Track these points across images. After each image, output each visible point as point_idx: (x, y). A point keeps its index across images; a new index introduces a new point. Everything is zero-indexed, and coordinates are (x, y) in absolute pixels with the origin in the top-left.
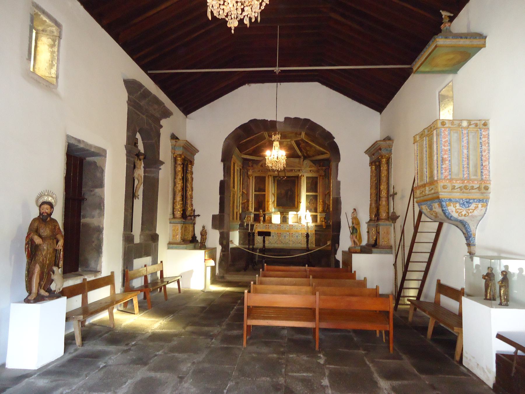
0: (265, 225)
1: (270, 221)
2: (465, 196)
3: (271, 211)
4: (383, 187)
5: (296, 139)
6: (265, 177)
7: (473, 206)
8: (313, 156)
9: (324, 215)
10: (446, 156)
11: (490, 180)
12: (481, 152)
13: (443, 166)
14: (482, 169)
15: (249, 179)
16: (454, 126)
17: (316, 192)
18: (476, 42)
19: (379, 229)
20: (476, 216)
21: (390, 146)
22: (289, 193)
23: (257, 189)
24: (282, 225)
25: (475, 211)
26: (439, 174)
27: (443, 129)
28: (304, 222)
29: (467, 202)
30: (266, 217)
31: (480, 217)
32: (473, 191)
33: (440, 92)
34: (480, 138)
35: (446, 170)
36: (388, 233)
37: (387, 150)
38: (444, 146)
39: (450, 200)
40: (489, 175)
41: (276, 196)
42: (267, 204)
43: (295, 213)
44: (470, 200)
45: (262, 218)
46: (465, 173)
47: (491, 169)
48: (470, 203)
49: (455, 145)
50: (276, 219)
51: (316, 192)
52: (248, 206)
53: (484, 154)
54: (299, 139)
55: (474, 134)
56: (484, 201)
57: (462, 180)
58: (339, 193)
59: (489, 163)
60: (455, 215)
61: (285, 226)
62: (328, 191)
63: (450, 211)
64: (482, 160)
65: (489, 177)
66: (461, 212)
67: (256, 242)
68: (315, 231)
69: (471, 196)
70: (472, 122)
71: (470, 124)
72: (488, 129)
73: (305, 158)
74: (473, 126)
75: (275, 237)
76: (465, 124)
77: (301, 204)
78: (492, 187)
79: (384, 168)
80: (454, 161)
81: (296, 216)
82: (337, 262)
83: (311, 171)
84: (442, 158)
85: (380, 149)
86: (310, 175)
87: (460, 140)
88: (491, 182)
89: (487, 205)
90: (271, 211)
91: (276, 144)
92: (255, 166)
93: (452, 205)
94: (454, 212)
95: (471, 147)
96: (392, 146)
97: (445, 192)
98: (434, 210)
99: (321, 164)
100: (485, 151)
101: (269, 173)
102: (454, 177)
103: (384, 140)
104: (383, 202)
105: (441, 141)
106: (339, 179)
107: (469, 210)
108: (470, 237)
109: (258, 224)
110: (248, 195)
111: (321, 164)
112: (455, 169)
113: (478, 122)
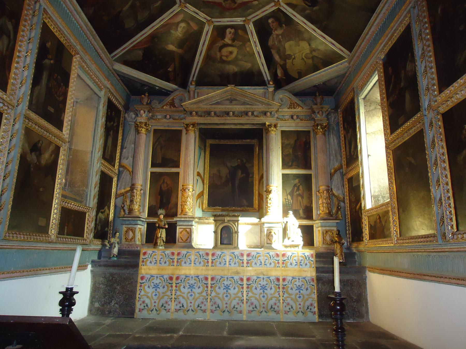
0: (168, 252)
3: (190, 214)
5: (259, 14)
6: (180, 132)
8: (301, 75)
9: (332, 225)
17: (307, 166)
22: (239, 174)
23: (159, 161)
24: (218, 252)
28: (278, 244)
30: (178, 230)
41: (207, 181)
42: (183, 195)
43: (255, 220)
45: (162, 234)
50: (204, 235)
51: (307, 166)
52: (132, 201)
54: (270, 8)
61: (227, 254)
62: (337, 165)
67: (138, 306)
68: (318, 270)
73: (279, 85)
75: (197, 290)
77: (271, 196)
81: (258, 229)
83: (292, 117)
86: (290, 126)
90: (190, 214)
92: (155, 104)
99: (319, 100)
101: (189, 120)
109: (150, 251)
110: (133, 173)
111: (319, 100)
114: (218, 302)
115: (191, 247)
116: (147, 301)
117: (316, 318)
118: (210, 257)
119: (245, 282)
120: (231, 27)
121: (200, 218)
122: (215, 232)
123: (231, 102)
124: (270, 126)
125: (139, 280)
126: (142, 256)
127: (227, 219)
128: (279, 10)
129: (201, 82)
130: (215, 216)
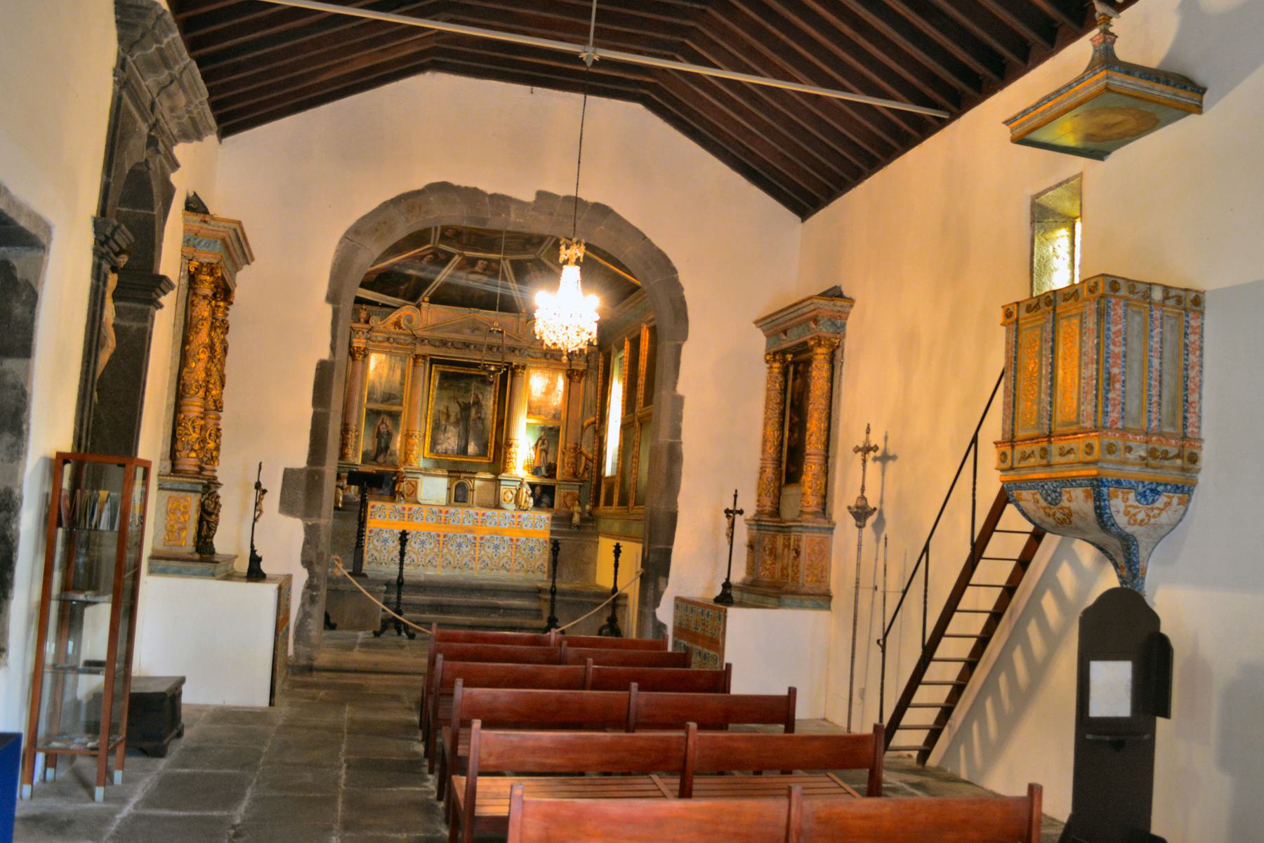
1: (412, 496)
2: (1148, 475)
4: (814, 425)
7: (1162, 500)
10: (1115, 370)
11: (1200, 440)
12: (1186, 369)
13: (1110, 395)
14: (1186, 411)
15: (354, 359)
16: (1136, 297)
18: (1184, 96)
19: (799, 540)
20: (1161, 526)
21: (843, 315)
24: (452, 510)
25: (1164, 514)
26: (1100, 415)
27: (1113, 301)
29: (1152, 490)
31: (1167, 529)
32: (1166, 463)
33: (1038, 195)
34: (1186, 334)
35: (1114, 405)
36: (823, 553)
37: (834, 324)
38: (1114, 344)
39: (1118, 482)
40: (1199, 427)
44: (1158, 484)
46: (1153, 416)
47: (1205, 414)
48: (1158, 493)
49: (1135, 344)
53: (1192, 373)
55: (1173, 322)
56: (1184, 489)
57: (1147, 434)
58: (677, 432)
59: (1200, 397)
60: (1121, 520)
63: (1113, 509)
64: (1186, 389)
65: (1199, 433)
66: (1135, 515)
67: (367, 558)
68: (552, 532)
69: (1162, 476)
70: (1172, 293)
71: (1166, 298)
72: (1202, 313)
74: (1172, 302)
75: (428, 546)
76: (1157, 295)
77: (512, 450)
78: (1206, 455)
79: (819, 373)
80: (1133, 385)
82: (660, 627)
84: (1109, 373)
85: (815, 321)
87: (1146, 333)
88: (1204, 446)
89: (1189, 501)
90: (415, 465)
91: (571, 274)
93: (1121, 495)
94: (1121, 514)
95: (1167, 355)
96: (848, 313)
97: (1110, 462)
98: (1065, 503)
100: (1193, 368)
102: (1130, 425)
103: (824, 295)
104: (812, 467)
105: (1109, 329)
106: (680, 389)
107: (1152, 509)
108: (1135, 576)
112: (1133, 405)
113: (1182, 293)
114: (450, 559)
115: (418, 503)
116: (376, 554)
117: (545, 577)
118: (443, 515)
119: (478, 541)
120: (485, 259)
121: (426, 469)
122: (449, 489)
123: (473, 331)
124: (517, 367)
125: (367, 533)
126: (370, 509)
127: (463, 475)
128: (540, 260)
129: (434, 300)
130: (450, 472)
